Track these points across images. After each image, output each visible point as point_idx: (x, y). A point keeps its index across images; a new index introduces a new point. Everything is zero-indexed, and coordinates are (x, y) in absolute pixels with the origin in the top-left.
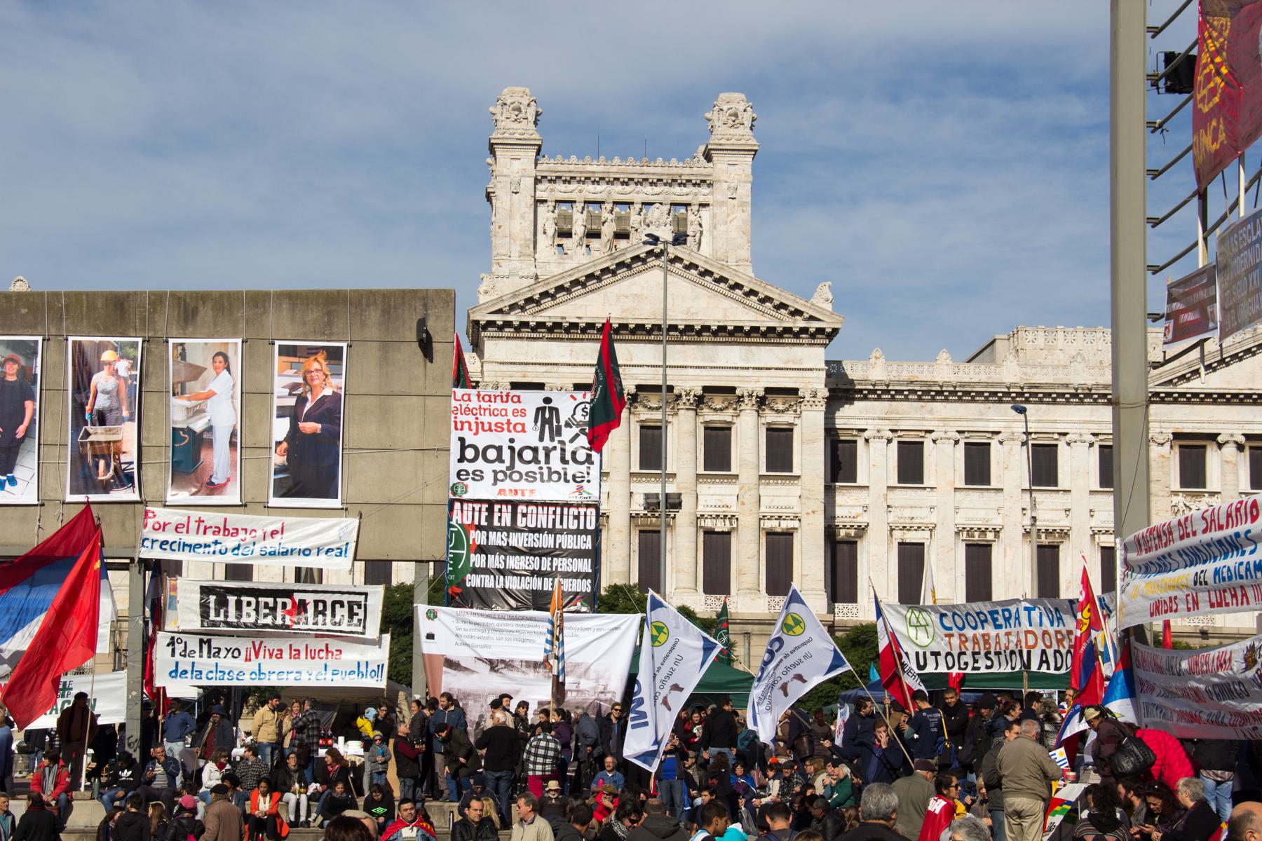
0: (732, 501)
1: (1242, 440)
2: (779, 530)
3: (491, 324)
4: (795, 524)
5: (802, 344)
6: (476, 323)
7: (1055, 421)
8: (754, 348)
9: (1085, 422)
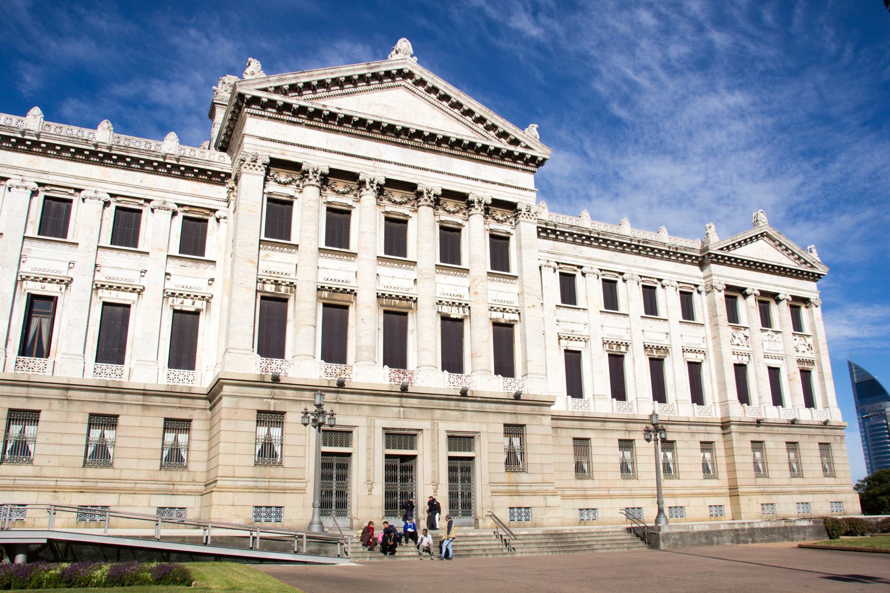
0: (464, 292)
1: (758, 293)
2: (503, 321)
3: (255, 100)
4: (515, 317)
5: (517, 169)
6: (241, 96)
7: (655, 270)
8: (481, 165)
9: (672, 273)
